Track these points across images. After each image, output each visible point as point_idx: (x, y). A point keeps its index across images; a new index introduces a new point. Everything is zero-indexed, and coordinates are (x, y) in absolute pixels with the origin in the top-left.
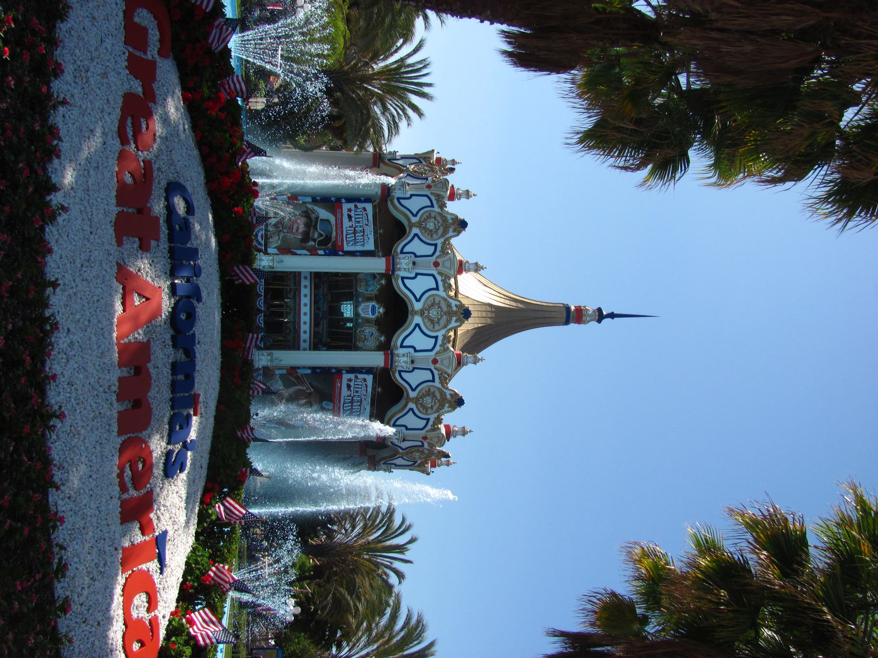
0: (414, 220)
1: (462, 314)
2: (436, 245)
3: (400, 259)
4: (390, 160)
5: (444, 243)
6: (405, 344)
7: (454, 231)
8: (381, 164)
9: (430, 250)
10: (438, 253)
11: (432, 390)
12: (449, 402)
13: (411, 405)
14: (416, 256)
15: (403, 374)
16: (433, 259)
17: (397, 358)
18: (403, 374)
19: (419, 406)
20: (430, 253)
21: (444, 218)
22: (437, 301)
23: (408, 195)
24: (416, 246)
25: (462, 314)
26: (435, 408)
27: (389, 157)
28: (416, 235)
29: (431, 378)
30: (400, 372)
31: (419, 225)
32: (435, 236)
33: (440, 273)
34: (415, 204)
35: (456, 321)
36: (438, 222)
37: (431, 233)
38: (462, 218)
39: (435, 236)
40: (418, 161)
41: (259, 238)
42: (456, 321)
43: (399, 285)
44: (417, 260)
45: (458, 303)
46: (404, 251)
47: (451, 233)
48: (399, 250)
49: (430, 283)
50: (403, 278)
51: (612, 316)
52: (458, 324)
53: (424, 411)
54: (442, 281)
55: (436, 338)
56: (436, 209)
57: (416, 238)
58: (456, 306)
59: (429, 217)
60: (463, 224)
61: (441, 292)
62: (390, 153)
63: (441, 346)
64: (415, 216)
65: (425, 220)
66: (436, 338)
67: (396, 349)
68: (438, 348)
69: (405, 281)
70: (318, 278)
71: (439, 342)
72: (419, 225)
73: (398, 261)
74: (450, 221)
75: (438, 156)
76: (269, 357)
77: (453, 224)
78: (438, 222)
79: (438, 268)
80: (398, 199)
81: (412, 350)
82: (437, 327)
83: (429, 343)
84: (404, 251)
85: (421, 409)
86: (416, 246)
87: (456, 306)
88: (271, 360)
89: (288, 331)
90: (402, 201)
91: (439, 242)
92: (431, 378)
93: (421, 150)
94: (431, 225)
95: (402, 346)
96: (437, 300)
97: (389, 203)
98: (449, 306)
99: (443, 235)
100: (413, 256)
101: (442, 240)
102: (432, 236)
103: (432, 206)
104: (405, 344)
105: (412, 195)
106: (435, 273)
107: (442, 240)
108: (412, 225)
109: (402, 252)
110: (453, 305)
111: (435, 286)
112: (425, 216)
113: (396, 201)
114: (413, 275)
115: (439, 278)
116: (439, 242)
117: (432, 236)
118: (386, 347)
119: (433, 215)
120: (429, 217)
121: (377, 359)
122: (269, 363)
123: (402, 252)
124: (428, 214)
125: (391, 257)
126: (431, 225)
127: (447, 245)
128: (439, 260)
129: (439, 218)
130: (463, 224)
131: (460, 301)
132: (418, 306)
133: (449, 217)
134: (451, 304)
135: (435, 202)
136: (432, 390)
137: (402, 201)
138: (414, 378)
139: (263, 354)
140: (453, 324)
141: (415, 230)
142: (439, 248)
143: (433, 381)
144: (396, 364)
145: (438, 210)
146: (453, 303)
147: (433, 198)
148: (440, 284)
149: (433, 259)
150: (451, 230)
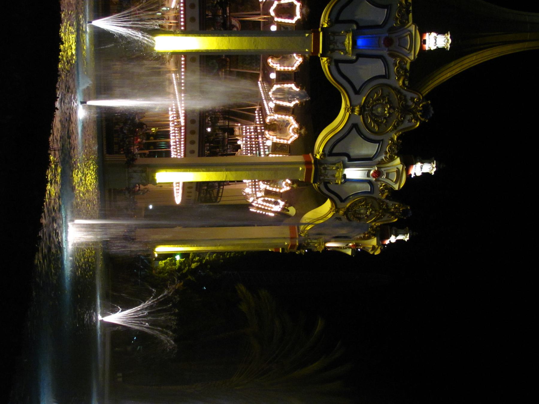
1: (420, 111)
25: (420, 111)
46: (341, 18)
69: (340, 65)
84: (341, 18)
95: (331, 154)
106: (385, 52)
110: (409, 98)
111: (383, 73)
115: (391, 60)
134: (405, 96)
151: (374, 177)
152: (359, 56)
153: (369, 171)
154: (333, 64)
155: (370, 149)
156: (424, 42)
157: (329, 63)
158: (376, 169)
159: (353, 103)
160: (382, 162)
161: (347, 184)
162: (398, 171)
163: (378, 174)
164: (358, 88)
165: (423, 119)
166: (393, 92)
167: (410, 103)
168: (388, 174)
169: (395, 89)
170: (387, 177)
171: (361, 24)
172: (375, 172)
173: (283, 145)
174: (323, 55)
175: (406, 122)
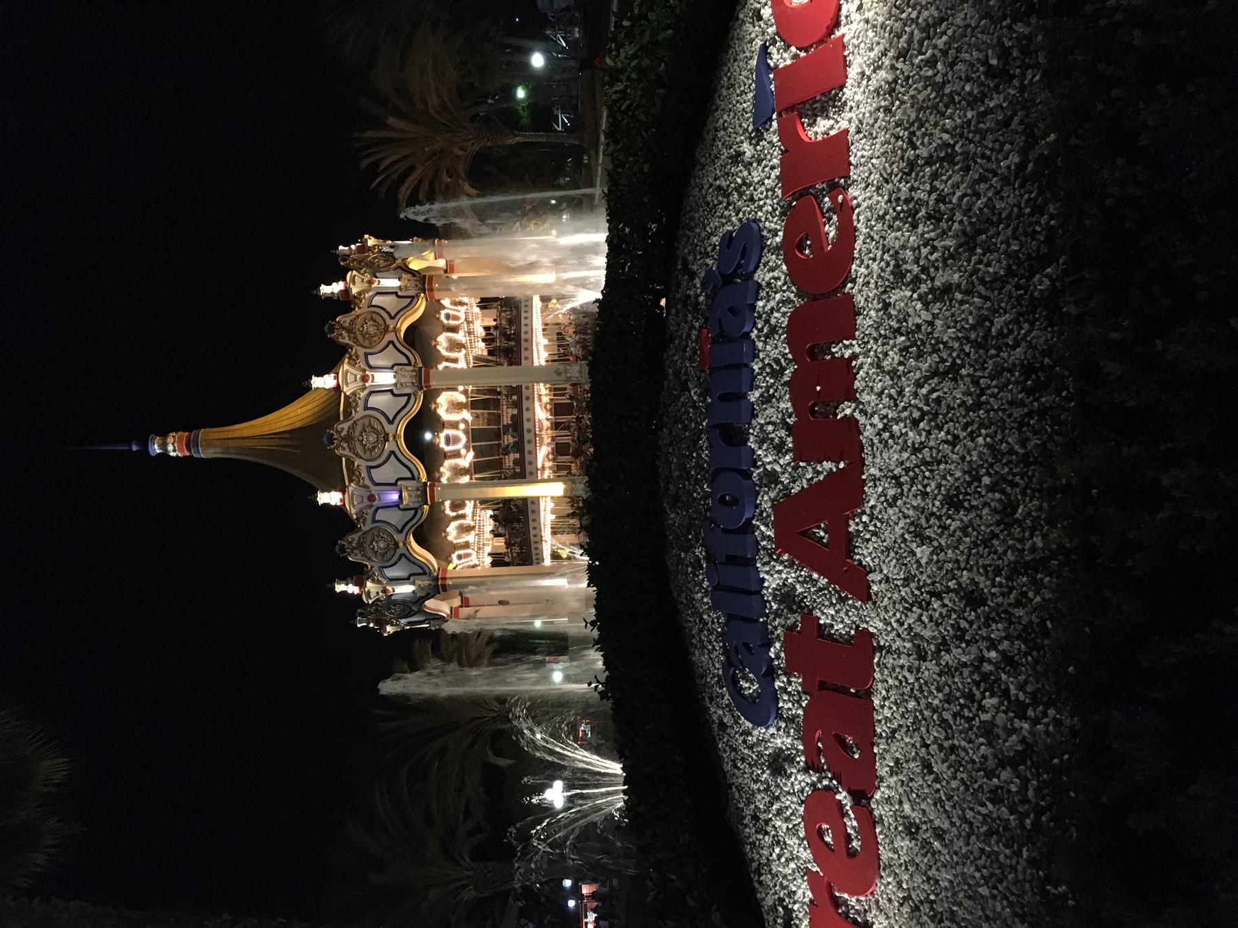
1: (335, 439)
6: (405, 398)
9: (381, 515)
10: (371, 511)
11: (367, 343)
12: (344, 328)
15: (406, 362)
16: (376, 503)
17: (414, 381)
18: (406, 362)
20: (380, 511)
22: (368, 453)
25: (335, 439)
28: (400, 532)
30: (409, 364)
32: (375, 532)
33: (365, 486)
49: (378, 475)
53: (375, 316)
69: (410, 476)
73: (420, 499)
76: (569, 375)
79: (369, 494)
82: (366, 422)
85: (380, 321)
88: (566, 371)
90: (422, 571)
95: (409, 395)
96: (368, 455)
98: (352, 449)
101: (365, 529)
104: (405, 398)
110: (347, 450)
114: (399, 483)
115: (368, 482)
122: (568, 367)
125: (429, 503)
128: (368, 503)
134: (350, 451)
137: (421, 571)
139: (577, 378)
142: (369, 518)
143: (366, 355)
144: (414, 374)
149: (376, 503)
151: (368, 375)
152: (395, 484)
153: (372, 381)
154: (416, 477)
155: (375, 401)
156: (343, 500)
157: (419, 478)
158: (367, 384)
159: (395, 443)
160: (364, 388)
161: (390, 364)
162: (347, 384)
163: (365, 379)
164: (393, 457)
165: (332, 432)
166: (361, 454)
167: (345, 445)
168: (356, 380)
169: (361, 458)
170: (356, 376)
171: (396, 508)
172: (367, 381)
173: (450, 457)
174: (420, 368)
175: (346, 428)
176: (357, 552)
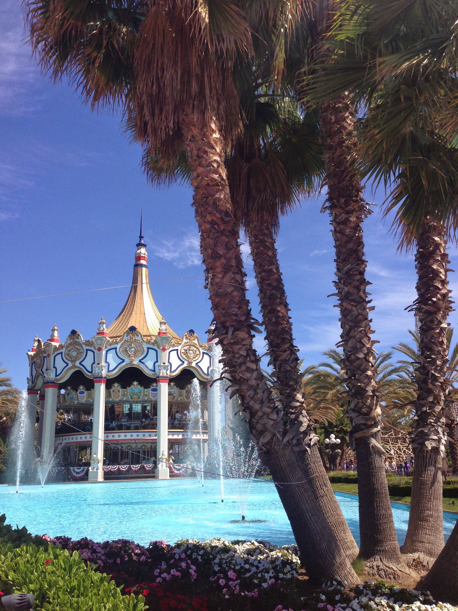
0: (70, 365)
2: (87, 350)
3: (95, 374)
4: (33, 383)
5: (86, 345)
7: (78, 338)
8: (35, 389)
9: (90, 354)
10: (92, 349)
11: (183, 351)
13: (194, 364)
14: (94, 363)
16: (96, 351)
19: (194, 359)
21: (70, 344)
23: (54, 369)
24: (88, 363)
26: (195, 349)
27: (31, 383)
28: (80, 363)
29: (176, 352)
31: (73, 361)
32: (81, 351)
34: (60, 364)
35: (137, 335)
36: (72, 349)
37: (79, 353)
38: (69, 333)
39: (81, 351)
40: (34, 365)
41: (79, 471)
42: (137, 335)
43: (114, 374)
44: (96, 362)
45: (126, 335)
46: (90, 371)
47: (80, 340)
48: (90, 374)
50: (109, 371)
51: (141, 237)
52: (139, 335)
54: (110, 345)
55: (148, 348)
56: (63, 350)
57: (83, 363)
58: (127, 336)
59: (68, 354)
60: (74, 332)
61: (118, 346)
62: (28, 383)
63: (154, 345)
64: (68, 364)
65: (71, 357)
66: (148, 348)
67: (155, 374)
68: (155, 347)
70: (107, 428)
71: (151, 346)
72: (73, 361)
74: (72, 341)
75: (31, 350)
77: (73, 339)
78: (72, 349)
80: (56, 376)
81: (157, 364)
83: (152, 353)
84: (90, 371)
86: (88, 363)
87: (127, 336)
89: (144, 447)
91: (85, 348)
92: (176, 352)
93: (27, 362)
94: (74, 354)
95: (154, 371)
97: (59, 382)
99: (81, 346)
100: (94, 365)
101: (84, 346)
102: (81, 353)
103: (61, 353)
105: (54, 367)
107: (84, 346)
108: (75, 367)
109: (91, 372)
112: (68, 358)
113: (58, 377)
116: (85, 348)
117: (81, 353)
118: (156, 380)
119: (67, 352)
120: (68, 354)
121: (164, 388)
123: (91, 372)
124: (67, 356)
126: (74, 354)
127: (88, 343)
129: (69, 348)
130: (74, 332)
131: (124, 334)
132: (127, 361)
133: (69, 342)
135: (59, 352)
136: (183, 351)
138: (175, 362)
140: (139, 338)
141: (77, 364)
142: (89, 348)
143: (177, 350)
145: (64, 349)
146: (125, 338)
147: (56, 353)
148: (113, 346)
149: (96, 351)
150: (77, 340)
176: (72, 341)
